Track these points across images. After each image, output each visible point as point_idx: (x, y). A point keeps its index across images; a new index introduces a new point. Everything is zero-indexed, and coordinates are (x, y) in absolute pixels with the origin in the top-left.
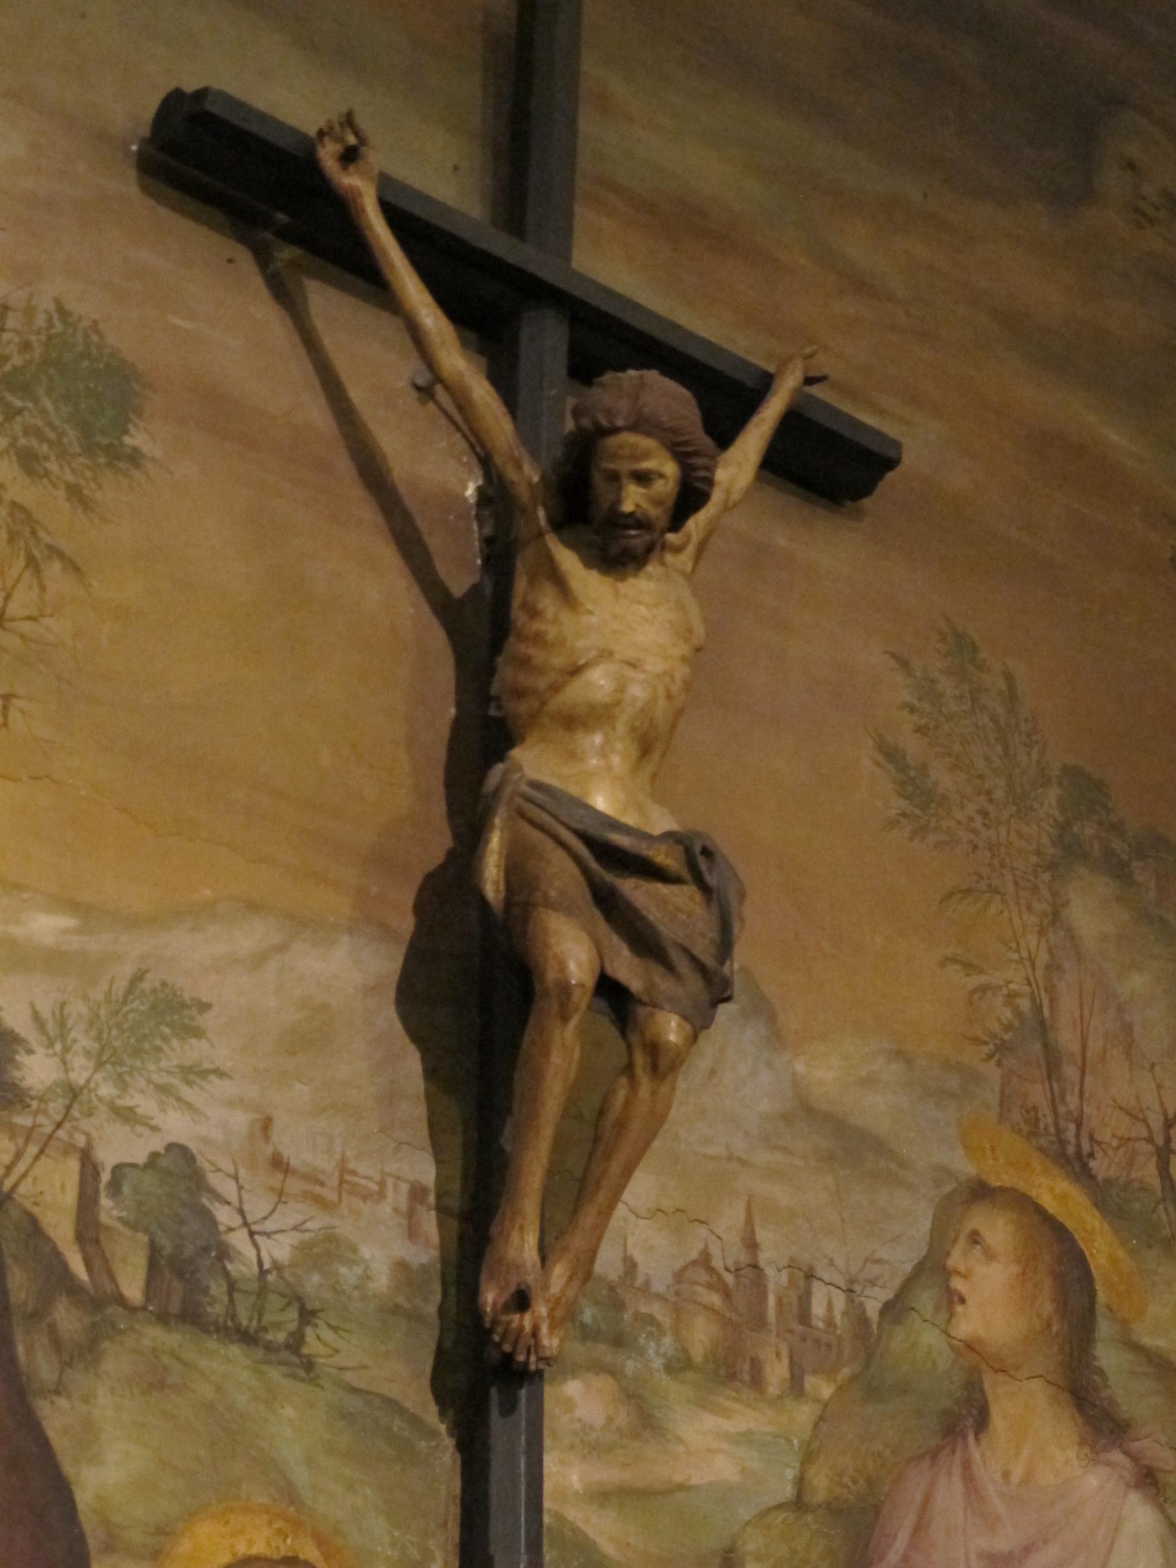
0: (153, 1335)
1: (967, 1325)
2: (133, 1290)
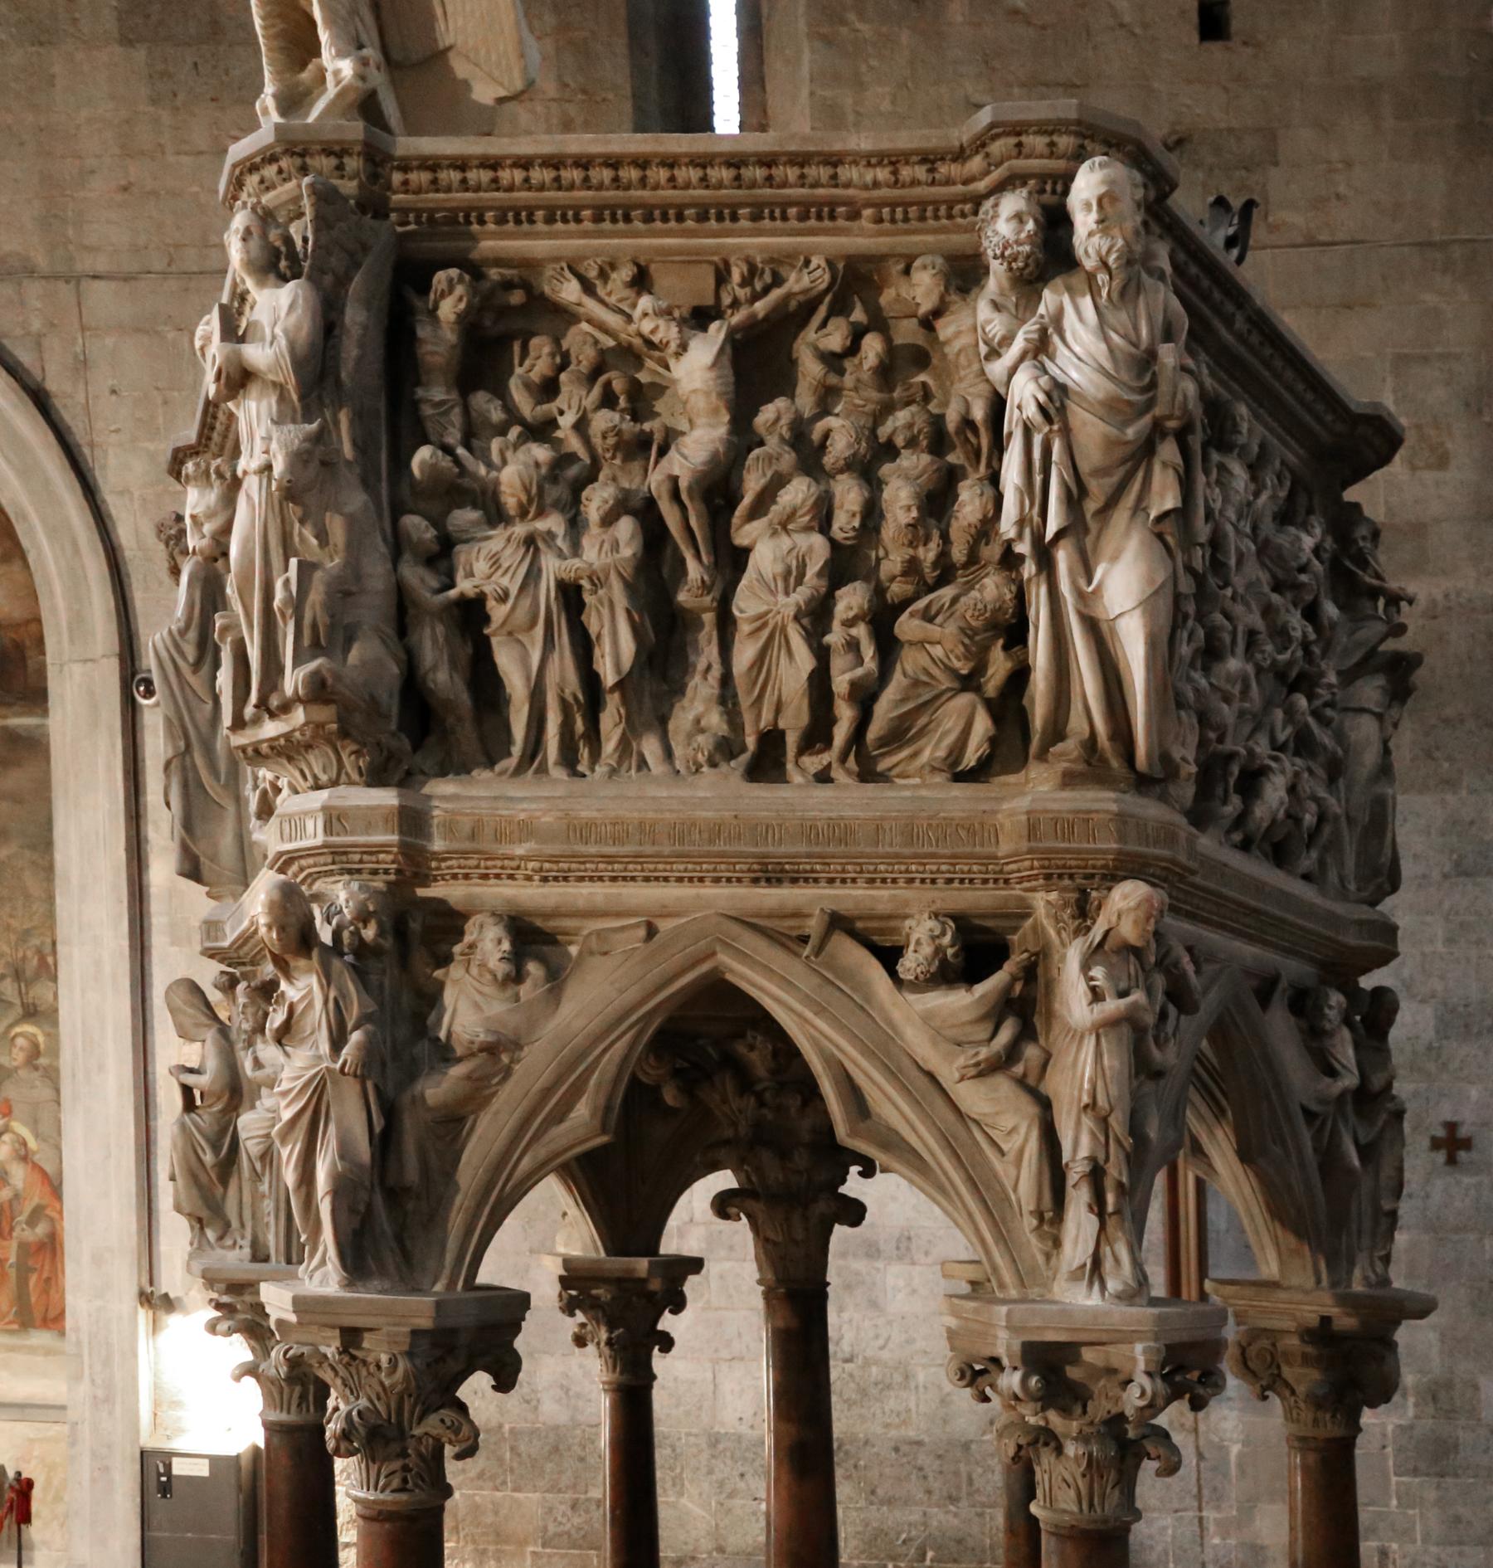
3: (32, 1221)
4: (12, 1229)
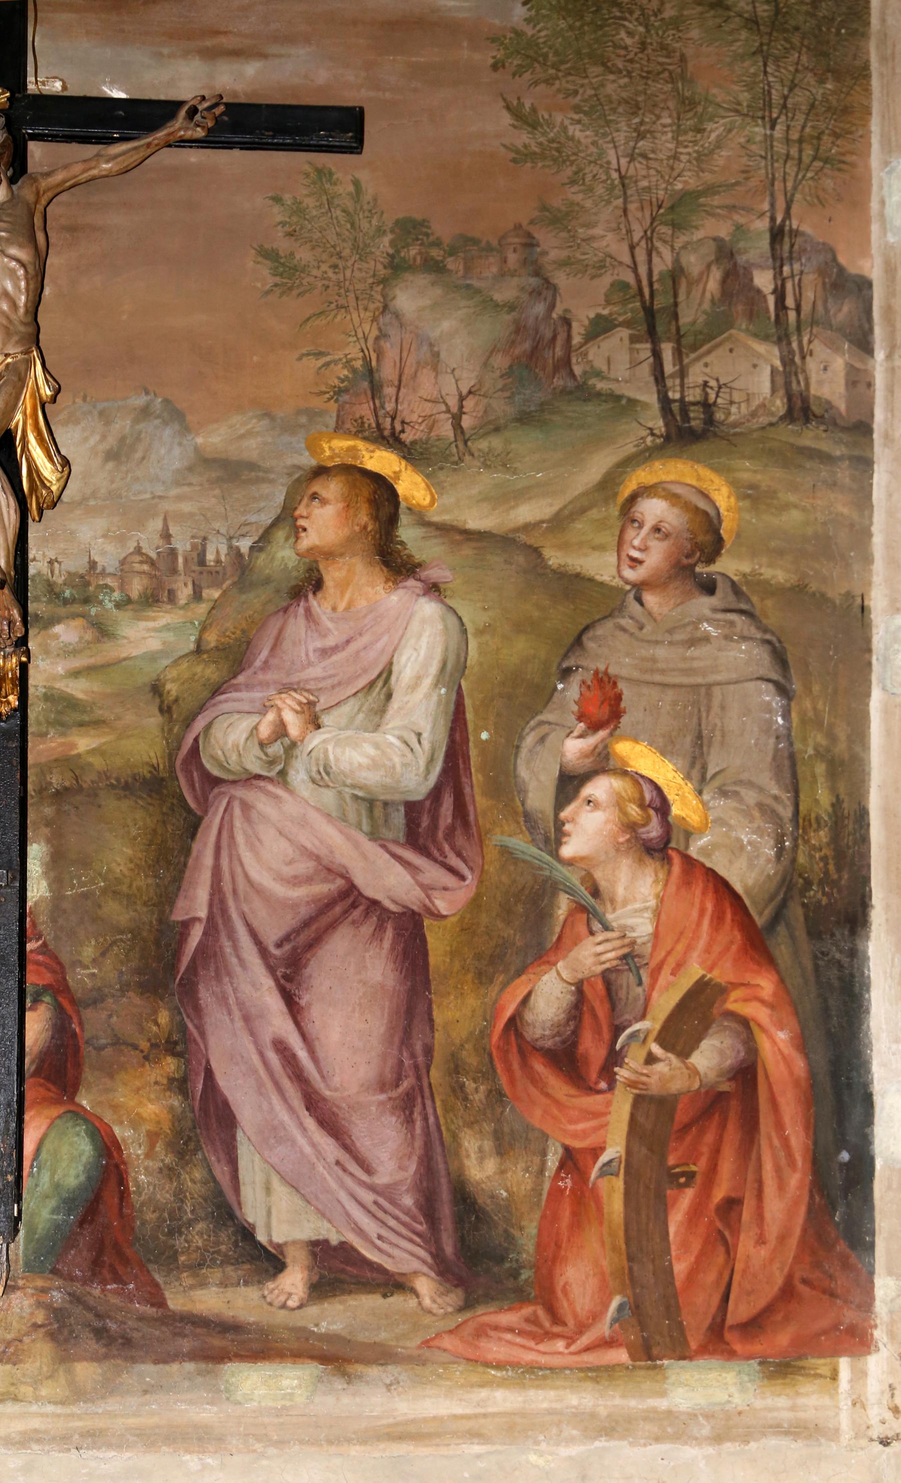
1: (308, 541)
3: (679, 1035)
4: (615, 1058)
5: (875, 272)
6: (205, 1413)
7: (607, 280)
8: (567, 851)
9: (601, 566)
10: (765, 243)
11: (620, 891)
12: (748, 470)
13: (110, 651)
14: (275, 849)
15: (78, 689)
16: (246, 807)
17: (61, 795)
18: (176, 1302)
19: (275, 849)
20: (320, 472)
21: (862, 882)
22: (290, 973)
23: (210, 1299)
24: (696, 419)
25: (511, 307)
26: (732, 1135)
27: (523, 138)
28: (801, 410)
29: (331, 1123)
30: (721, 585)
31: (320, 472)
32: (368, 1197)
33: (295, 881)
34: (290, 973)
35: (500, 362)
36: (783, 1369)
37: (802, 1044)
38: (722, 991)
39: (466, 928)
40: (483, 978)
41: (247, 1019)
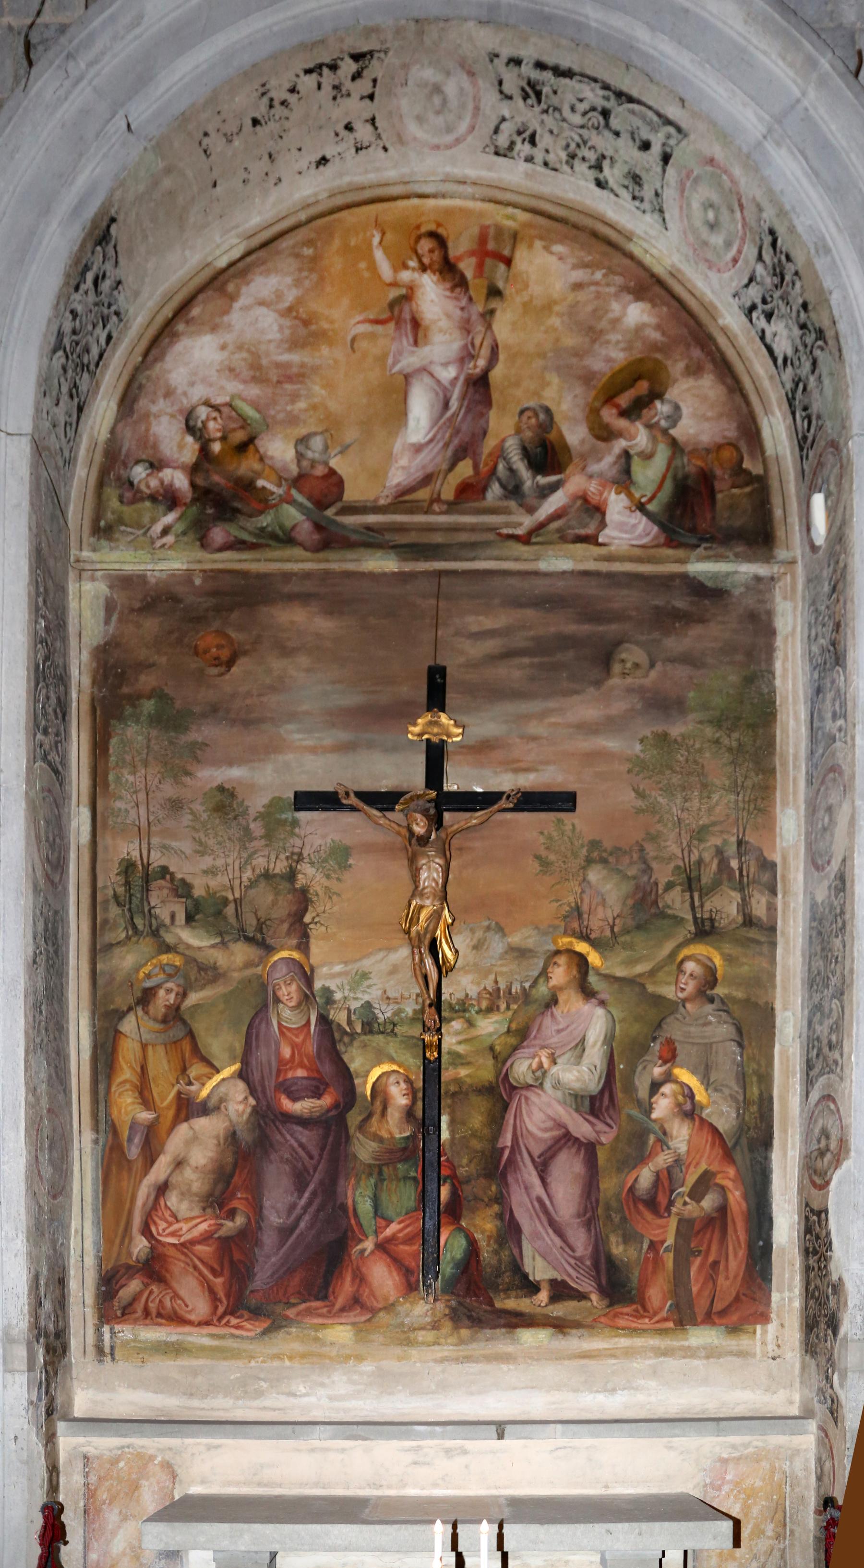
0: (363, 1037)
1: (553, 982)
2: (359, 1030)
3: (697, 1193)
4: (671, 1203)
5: (778, 860)
6: (510, 1349)
7: (672, 865)
8: (654, 1116)
9: (669, 992)
10: (734, 847)
11: (675, 1133)
12: (728, 948)
13: (474, 1032)
14: (538, 1116)
15: (461, 1049)
16: (527, 1099)
17: (454, 1095)
18: (498, 1305)
19: (538, 1116)
20: (558, 952)
21: (770, 1127)
22: (543, 1168)
23: (510, 1304)
24: (707, 927)
25: (634, 878)
26: (717, 1235)
27: (640, 803)
28: (749, 921)
29: (559, 1232)
30: (717, 1001)
31: (558, 952)
32: (572, 1261)
33: (546, 1130)
34: (543, 1168)
35: (630, 902)
36: (734, 1330)
37: (745, 1197)
38: (714, 1174)
39: (613, 1148)
40: (619, 1170)
41: (526, 1188)
